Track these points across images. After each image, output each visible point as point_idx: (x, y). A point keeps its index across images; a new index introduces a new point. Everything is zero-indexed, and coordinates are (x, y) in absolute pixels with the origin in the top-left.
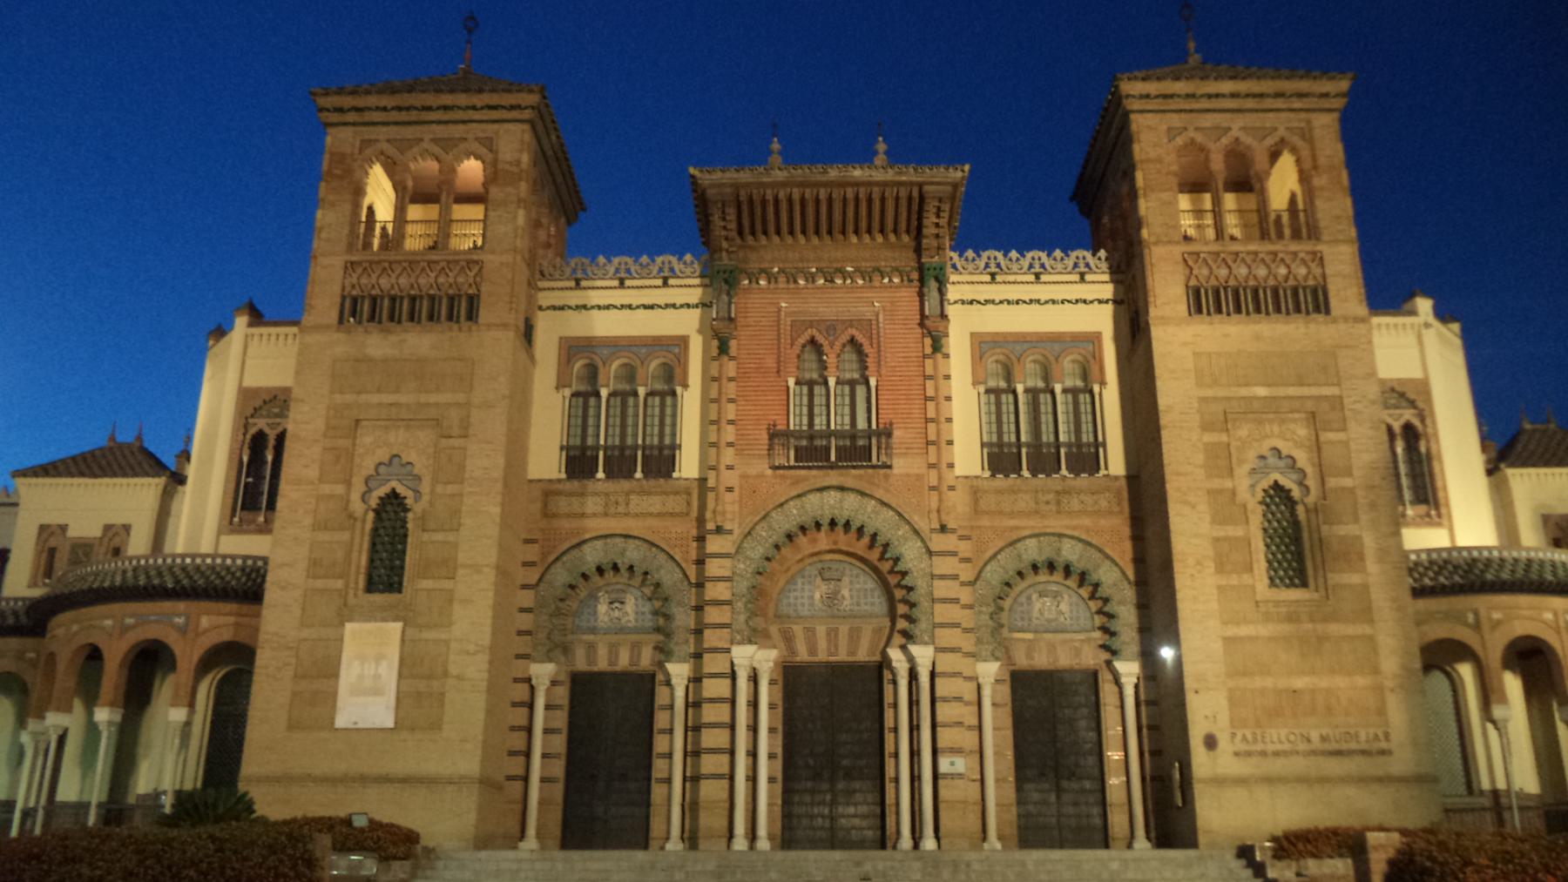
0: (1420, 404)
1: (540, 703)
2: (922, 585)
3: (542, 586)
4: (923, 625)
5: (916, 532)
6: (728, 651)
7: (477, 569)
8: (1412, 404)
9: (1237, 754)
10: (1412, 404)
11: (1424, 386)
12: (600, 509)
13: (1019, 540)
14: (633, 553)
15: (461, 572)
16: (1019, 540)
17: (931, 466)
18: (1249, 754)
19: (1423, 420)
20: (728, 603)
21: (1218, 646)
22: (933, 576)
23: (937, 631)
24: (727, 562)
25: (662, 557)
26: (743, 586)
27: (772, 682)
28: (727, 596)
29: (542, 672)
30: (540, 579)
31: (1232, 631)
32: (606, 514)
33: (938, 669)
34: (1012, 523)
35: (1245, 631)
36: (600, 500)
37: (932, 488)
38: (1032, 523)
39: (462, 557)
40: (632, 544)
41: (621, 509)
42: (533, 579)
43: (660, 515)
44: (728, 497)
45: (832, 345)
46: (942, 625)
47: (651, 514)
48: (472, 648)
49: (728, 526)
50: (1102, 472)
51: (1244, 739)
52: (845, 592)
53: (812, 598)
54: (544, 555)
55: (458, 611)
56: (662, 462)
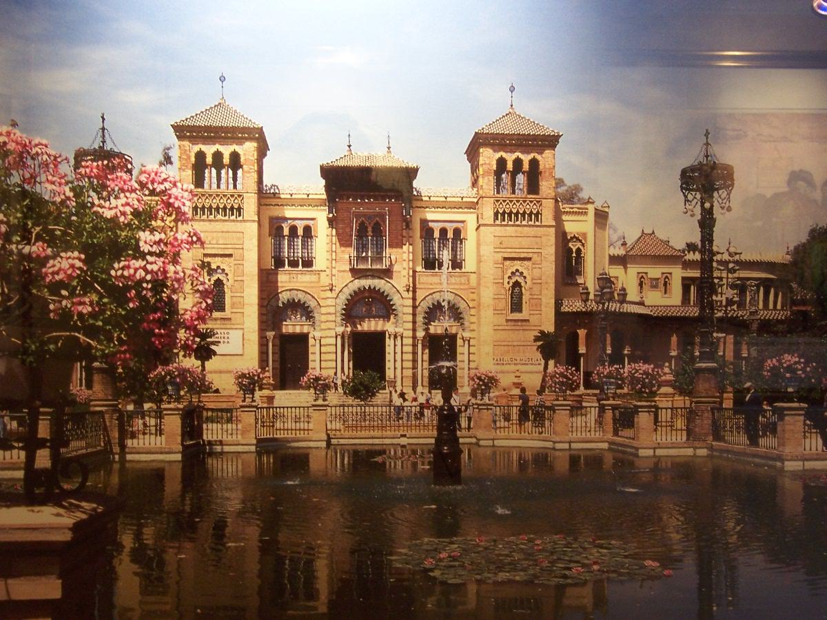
0: (583, 241)
1: (270, 344)
2: (399, 309)
3: (269, 306)
4: (400, 322)
5: (398, 291)
6: (335, 329)
7: (251, 305)
8: (580, 241)
9: (494, 364)
10: (580, 241)
11: (584, 235)
12: (288, 280)
13: (434, 293)
14: (300, 296)
15: (245, 306)
16: (434, 293)
17: (405, 269)
18: (498, 364)
19: (584, 246)
20: (335, 314)
21: (492, 332)
22: (404, 306)
23: (404, 324)
24: (334, 300)
25: (310, 297)
26: (339, 308)
27: (349, 338)
28: (334, 312)
29: (270, 334)
30: (268, 304)
31: (496, 328)
32: (290, 282)
33: (404, 335)
34: (431, 287)
35: (500, 328)
36: (288, 276)
37: (404, 276)
38: (437, 287)
39: (246, 301)
40: (299, 292)
41: (294, 280)
42: (265, 304)
43: (308, 282)
44: (333, 278)
45: (370, 223)
46: (406, 322)
47: (305, 282)
48: (252, 331)
49: (334, 288)
50: (463, 270)
51: (497, 360)
52: (374, 309)
53: (362, 310)
54: (268, 296)
55: (246, 319)
56: (308, 263)
